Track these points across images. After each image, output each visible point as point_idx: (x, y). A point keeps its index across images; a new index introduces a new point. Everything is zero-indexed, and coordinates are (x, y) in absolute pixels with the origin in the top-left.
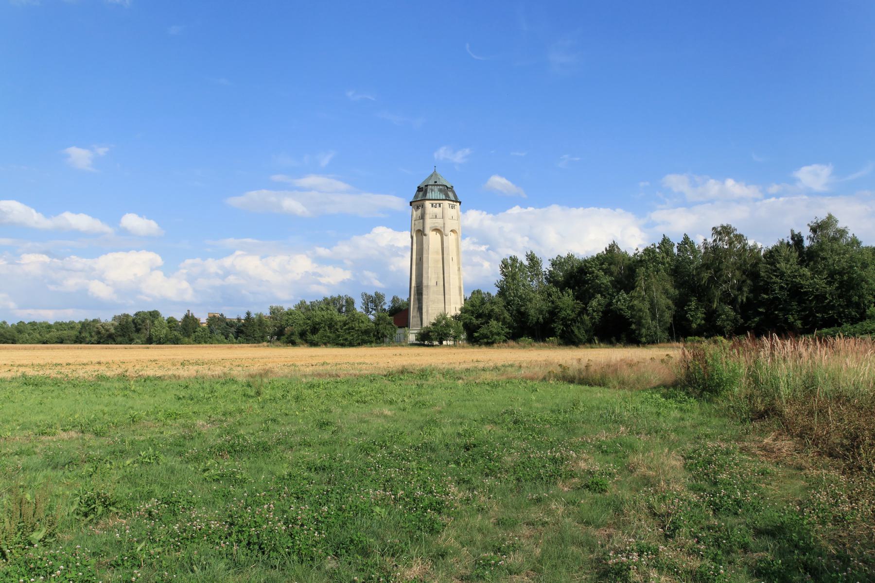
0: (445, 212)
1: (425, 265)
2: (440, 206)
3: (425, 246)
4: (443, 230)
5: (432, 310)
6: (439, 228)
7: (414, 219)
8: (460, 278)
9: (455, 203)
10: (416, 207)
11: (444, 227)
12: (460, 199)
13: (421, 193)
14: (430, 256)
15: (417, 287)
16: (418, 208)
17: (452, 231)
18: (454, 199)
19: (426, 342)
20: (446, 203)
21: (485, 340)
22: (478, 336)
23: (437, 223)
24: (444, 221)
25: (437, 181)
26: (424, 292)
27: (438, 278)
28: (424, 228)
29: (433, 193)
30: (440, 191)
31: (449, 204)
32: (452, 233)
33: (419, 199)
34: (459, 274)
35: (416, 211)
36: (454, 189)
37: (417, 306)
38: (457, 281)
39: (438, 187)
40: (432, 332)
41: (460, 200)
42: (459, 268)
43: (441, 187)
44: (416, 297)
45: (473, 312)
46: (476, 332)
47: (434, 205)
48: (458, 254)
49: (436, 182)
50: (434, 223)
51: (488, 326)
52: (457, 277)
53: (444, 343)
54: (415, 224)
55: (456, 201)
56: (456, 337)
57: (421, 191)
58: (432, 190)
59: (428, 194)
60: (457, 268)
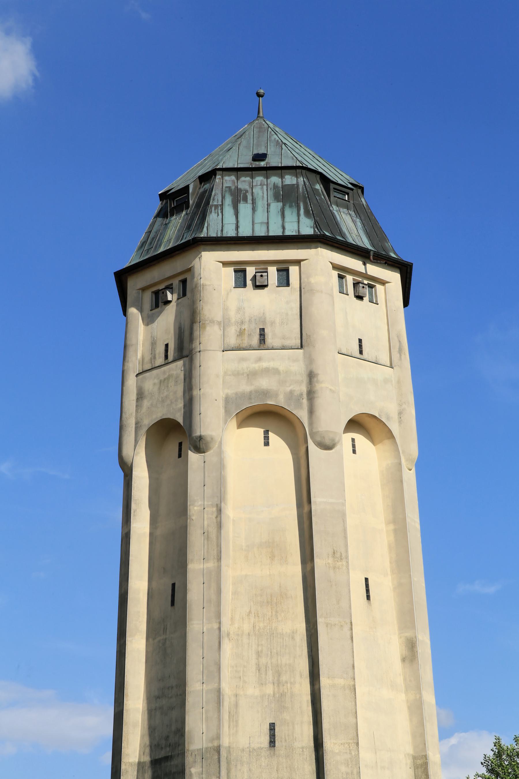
4: (303, 415)
6: (281, 401)
10: (148, 298)
11: (311, 394)
15: (155, 763)
18: (365, 243)
23: (267, 371)
24: (310, 360)
25: (271, 150)
29: (245, 208)
32: (360, 439)
35: (149, 320)
39: (275, 180)
43: (289, 180)
47: (251, 271)
49: (259, 157)
50: (252, 375)
54: (140, 396)
59: (213, 218)
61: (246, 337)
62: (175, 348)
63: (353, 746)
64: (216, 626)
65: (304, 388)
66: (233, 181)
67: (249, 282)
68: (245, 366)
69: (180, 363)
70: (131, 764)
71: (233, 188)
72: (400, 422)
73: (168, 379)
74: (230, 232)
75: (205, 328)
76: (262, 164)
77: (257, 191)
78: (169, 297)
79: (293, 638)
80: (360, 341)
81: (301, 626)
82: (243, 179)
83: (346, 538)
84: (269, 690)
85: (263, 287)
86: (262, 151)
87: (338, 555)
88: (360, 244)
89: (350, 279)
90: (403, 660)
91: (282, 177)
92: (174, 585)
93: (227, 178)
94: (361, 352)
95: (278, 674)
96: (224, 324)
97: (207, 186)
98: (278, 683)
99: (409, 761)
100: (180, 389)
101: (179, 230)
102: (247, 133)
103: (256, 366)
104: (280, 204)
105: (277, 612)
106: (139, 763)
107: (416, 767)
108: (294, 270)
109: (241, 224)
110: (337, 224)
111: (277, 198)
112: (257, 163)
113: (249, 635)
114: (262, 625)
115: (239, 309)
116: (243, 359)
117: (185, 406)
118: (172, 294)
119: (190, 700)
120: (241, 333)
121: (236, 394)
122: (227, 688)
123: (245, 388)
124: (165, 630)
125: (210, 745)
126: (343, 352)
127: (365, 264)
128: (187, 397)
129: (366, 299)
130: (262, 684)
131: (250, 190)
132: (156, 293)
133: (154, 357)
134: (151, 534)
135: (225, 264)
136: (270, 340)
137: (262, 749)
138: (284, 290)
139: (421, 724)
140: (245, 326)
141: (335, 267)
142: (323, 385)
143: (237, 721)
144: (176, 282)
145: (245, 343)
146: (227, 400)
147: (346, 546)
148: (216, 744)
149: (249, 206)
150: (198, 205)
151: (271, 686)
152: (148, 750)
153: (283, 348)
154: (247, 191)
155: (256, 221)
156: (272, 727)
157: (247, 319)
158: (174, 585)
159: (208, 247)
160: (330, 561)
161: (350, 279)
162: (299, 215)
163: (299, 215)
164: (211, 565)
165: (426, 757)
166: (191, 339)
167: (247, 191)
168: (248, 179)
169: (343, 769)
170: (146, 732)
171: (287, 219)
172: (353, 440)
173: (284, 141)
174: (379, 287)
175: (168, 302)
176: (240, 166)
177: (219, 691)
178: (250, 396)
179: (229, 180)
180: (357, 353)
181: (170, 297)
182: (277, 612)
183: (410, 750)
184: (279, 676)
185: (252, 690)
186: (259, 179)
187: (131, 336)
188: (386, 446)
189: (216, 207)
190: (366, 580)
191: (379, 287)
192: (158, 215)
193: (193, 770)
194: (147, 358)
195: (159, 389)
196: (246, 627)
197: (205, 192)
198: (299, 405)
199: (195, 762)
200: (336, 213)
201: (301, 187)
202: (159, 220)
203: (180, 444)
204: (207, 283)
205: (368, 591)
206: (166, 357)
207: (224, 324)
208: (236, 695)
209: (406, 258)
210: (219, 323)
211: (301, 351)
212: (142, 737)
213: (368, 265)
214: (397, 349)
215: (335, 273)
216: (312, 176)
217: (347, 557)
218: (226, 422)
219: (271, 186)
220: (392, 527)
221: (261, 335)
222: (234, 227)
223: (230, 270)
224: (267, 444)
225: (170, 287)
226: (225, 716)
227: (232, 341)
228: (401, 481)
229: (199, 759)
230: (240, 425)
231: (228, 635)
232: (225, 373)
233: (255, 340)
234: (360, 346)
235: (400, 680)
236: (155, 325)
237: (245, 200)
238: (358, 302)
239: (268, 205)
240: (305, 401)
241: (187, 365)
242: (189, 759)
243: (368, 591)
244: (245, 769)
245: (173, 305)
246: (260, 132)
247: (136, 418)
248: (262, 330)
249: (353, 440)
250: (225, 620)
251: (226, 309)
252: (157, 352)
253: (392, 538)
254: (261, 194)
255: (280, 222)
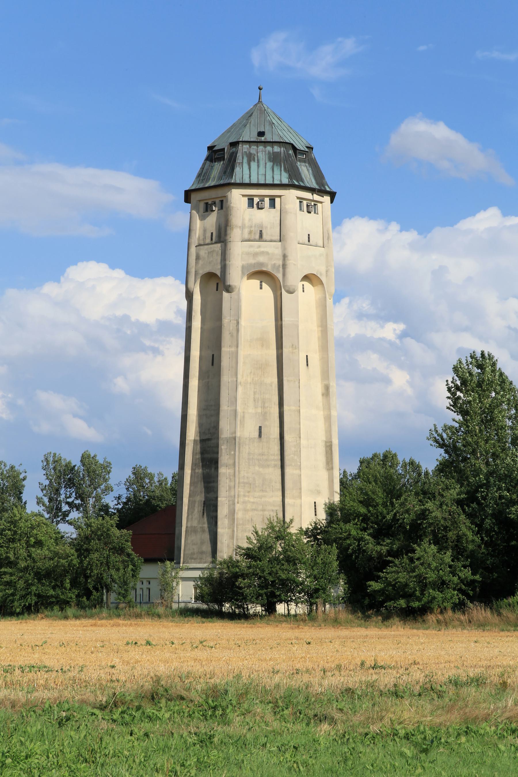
0: (289, 221)
1: (226, 378)
2: (273, 205)
3: (227, 321)
4: (280, 276)
5: (246, 510)
6: (269, 269)
7: (195, 241)
8: (328, 419)
9: (316, 197)
10: (202, 206)
11: (284, 266)
12: (332, 185)
13: (218, 167)
14: (243, 352)
15: (202, 441)
16: (208, 208)
17: (306, 278)
19: (227, 607)
20: (293, 194)
21: (402, 603)
22: (382, 592)
23: (263, 253)
24: (284, 248)
25: (267, 129)
26: (224, 458)
27: (264, 415)
28: (224, 268)
29: (254, 165)
30: (275, 159)
31: (301, 200)
32: (306, 284)
33: (211, 183)
34: (328, 407)
35: (203, 218)
36: (316, 154)
37: (200, 498)
38: (321, 425)
39: (269, 148)
40: (243, 576)
41: (332, 186)
42: (327, 388)
43: (277, 149)
44: (199, 471)
45: (365, 519)
46: (377, 579)
47: (256, 200)
48: (324, 347)
49: (261, 134)
50: (256, 255)
51: (411, 560)
52: (320, 414)
53: (281, 608)
54: (198, 258)
55: (322, 192)
56: (317, 590)
57: (219, 159)
58: (251, 158)
59: (237, 170)
60: (319, 389)
61: (253, 234)
62: (216, 236)
63: (298, 439)
64: (235, 379)
65: (281, 263)
66: (248, 148)
67: (255, 206)
68: (252, 250)
69: (219, 245)
70: (191, 440)
71: (248, 152)
72: (327, 276)
73: (213, 251)
74: (247, 181)
75: (233, 229)
76: (263, 139)
77: (260, 154)
78: (214, 208)
79: (271, 386)
80: (309, 235)
81: (275, 380)
82: (253, 147)
83: (298, 338)
84: (259, 410)
85: (262, 209)
86: (262, 130)
87: (294, 346)
88: (312, 187)
89: (305, 203)
90: (323, 395)
91: (273, 148)
92: (213, 355)
93: (244, 146)
94: (309, 241)
95: (264, 403)
96: (243, 227)
97: (234, 149)
98: (263, 407)
99: (324, 444)
100: (219, 259)
101: (219, 173)
102: (254, 114)
103: (257, 250)
104: (272, 164)
105: (264, 373)
106: (194, 440)
107: (326, 447)
108: (277, 200)
109: (251, 175)
110: (300, 174)
111: (270, 160)
112: (260, 138)
113: (250, 383)
114: (256, 379)
115: (250, 220)
116: (251, 246)
117: (221, 268)
118: (215, 207)
119: (222, 414)
120: (250, 232)
121: (248, 264)
122: (239, 409)
123: (252, 261)
124: (208, 377)
125: (231, 436)
126: (301, 242)
127: (313, 195)
128: (223, 264)
129: (313, 213)
130: (256, 407)
131: (256, 154)
132: (207, 204)
133: (205, 238)
134: (201, 328)
135: (244, 196)
136: (265, 236)
137: (255, 438)
138: (272, 210)
139: (330, 426)
140: (253, 229)
141: (298, 198)
142: (290, 262)
143: (244, 425)
144: (217, 201)
145: (252, 238)
146: (243, 267)
147: (298, 342)
148: (234, 436)
149: (256, 164)
150: (230, 160)
151: (260, 409)
152: (198, 435)
153: (271, 241)
154: (255, 155)
155: (259, 173)
156: (260, 428)
157: (254, 225)
158: (213, 355)
159: (234, 187)
160: (291, 349)
161: (305, 203)
162: (281, 171)
163: (281, 171)
164: (233, 349)
165: (331, 442)
166: (226, 234)
167: (255, 155)
168: (255, 147)
169: (293, 449)
170: (197, 425)
171: (275, 173)
172: (303, 285)
173: (274, 121)
174: (319, 205)
175: (213, 211)
176: (252, 140)
177: (236, 411)
178: (254, 265)
179: (246, 147)
180: (307, 242)
181: (214, 209)
182: (264, 373)
183: (324, 439)
184: (264, 404)
185: (251, 410)
186: (261, 148)
187: (193, 225)
188: (319, 287)
189: (239, 163)
190: (307, 356)
191: (319, 205)
192: (207, 159)
193: (223, 447)
194: (201, 238)
195: (208, 256)
196: (249, 380)
197: (233, 153)
198: (278, 271)
199: (224, 443)
200: (299, 166)
201: (282, 154)
202: (208, 162)
203: (217, 284)
204: (235, 206)
205: (307, 362)
206: (212, 239)
207: (243, 227)
208: (244, 412)
209: (334, 190)
210: (240, 227)
211: (280, 243)
212: (196, 427)
213: (315, 195)
214: (327, 238)
215: (298, 201)
216: (287, 146)
217: (298, 348)
218: (242, 278)
219: (267, 152)
220: (320, 329)
221: (260, 233)
222: (248, 176)
223: (246, 199)
224: (261, 288)
225: (214, 203)
226: (238, 422)
227: (246, 236)
228: (326, 306)
229: (225, 442)
230: (248, 278)
231: (241, 383)
232: (242, 253)
233: (257, 236)
234: (309, 238)
235: (321, 405)
236: (206, 221)
237: (254, 160)
238: (309, 214)
239: (266, 164)
240: (281, 269)
241: (223, 246)
242: (221, 442)
243: (307, 362)
244: (247, 447)
245: (216, 212)
246: (260, 113)
247: (195, 269)
248: (261, 231)
249: (303, 285)
250: (239, 376)
251: (243, 220)
252: (207, 235)
253: (320, 334)
254: (262, 157)
255: (272, 174)
